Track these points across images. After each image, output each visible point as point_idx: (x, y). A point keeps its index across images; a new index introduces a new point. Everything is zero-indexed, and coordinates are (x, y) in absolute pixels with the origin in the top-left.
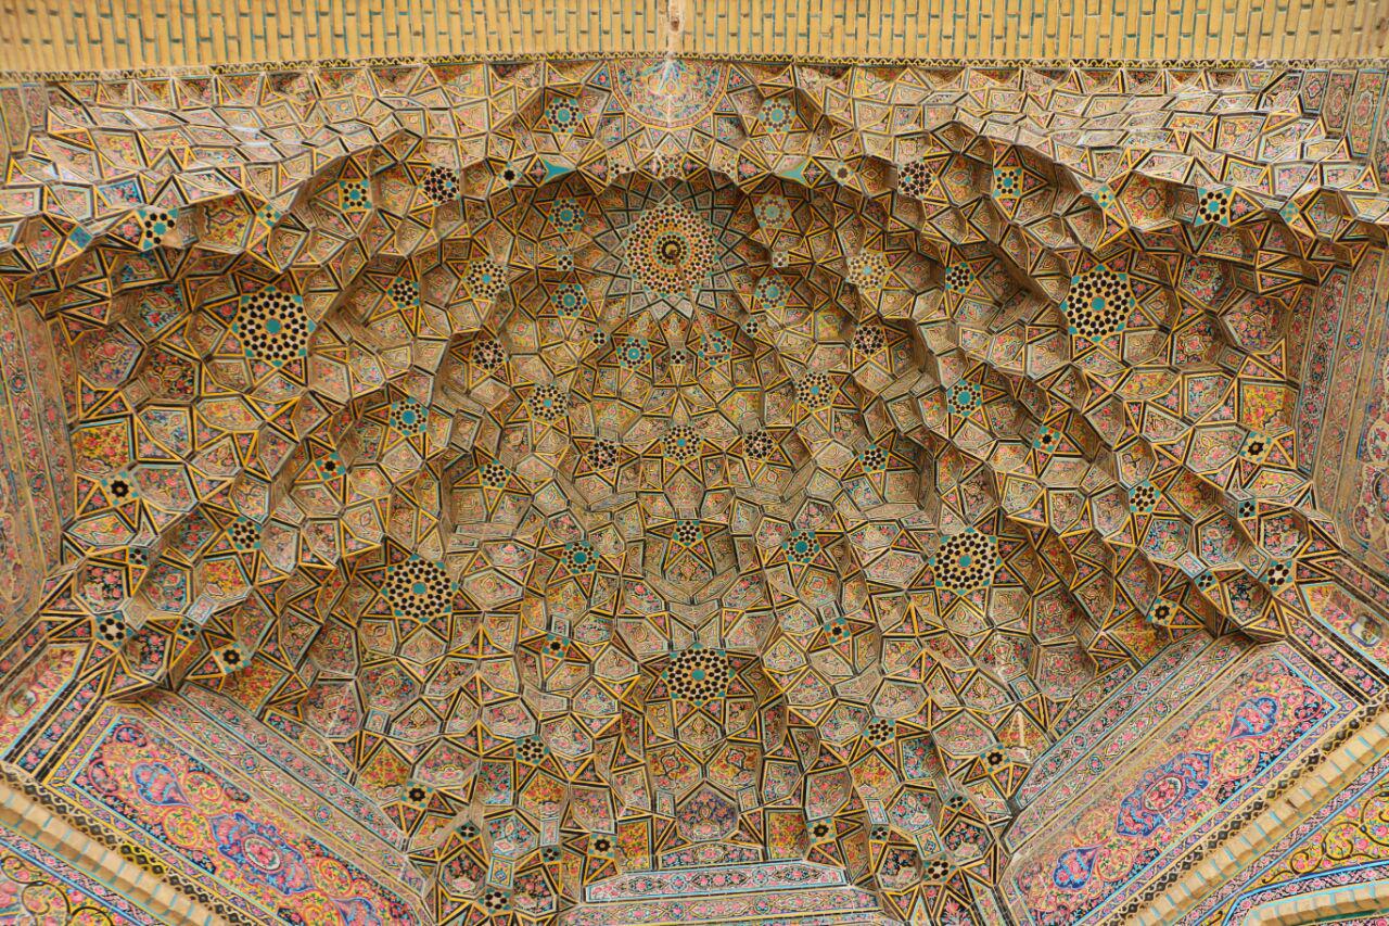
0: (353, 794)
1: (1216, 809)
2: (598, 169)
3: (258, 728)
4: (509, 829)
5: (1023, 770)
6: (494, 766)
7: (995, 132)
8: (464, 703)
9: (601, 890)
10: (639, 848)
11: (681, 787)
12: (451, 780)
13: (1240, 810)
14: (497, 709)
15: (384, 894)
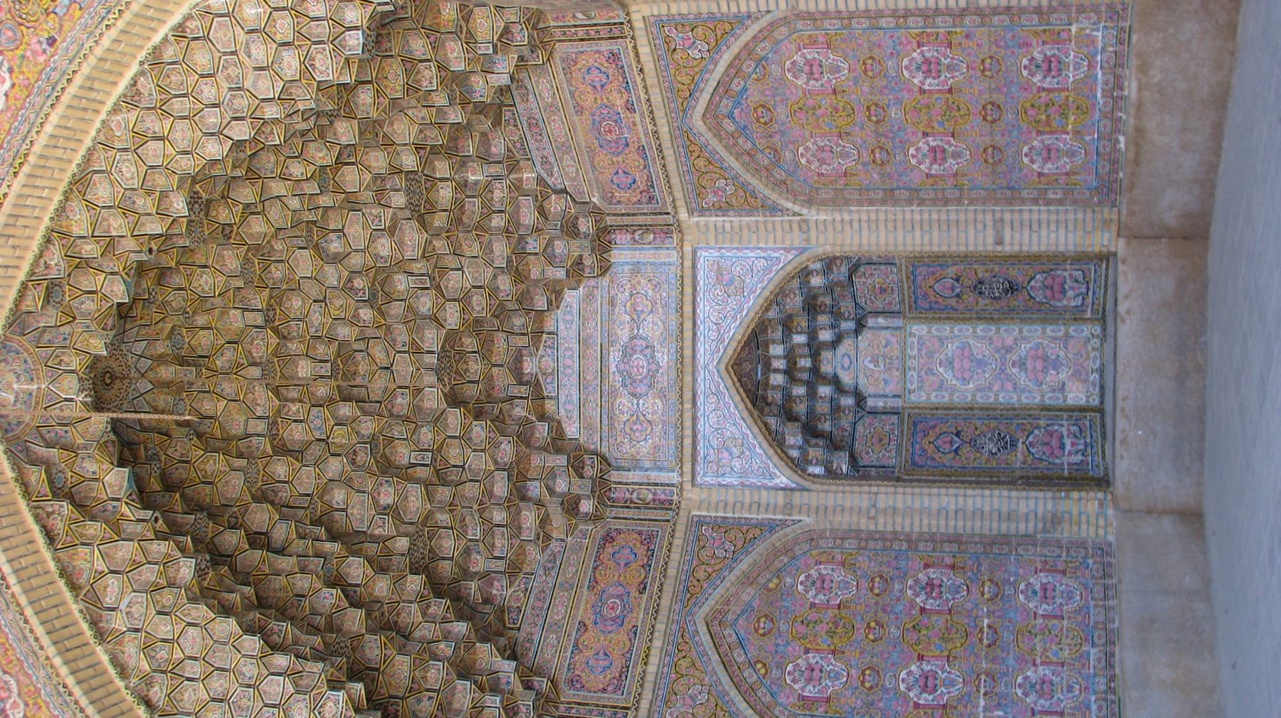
0: (541, 572)
1: (637, 116)
2: (111, 449)
3: (526, 628)
4: (550, 483)
5: (540, 181)
6: (519, 494)
7: (214, 149)
8: (486, 515)
9: (571, 430)
10: (542, 406)
11: (503, 378)
12: (529, 518)
13: (645, 107)
14: (491, 494)
15: (602, 547)
